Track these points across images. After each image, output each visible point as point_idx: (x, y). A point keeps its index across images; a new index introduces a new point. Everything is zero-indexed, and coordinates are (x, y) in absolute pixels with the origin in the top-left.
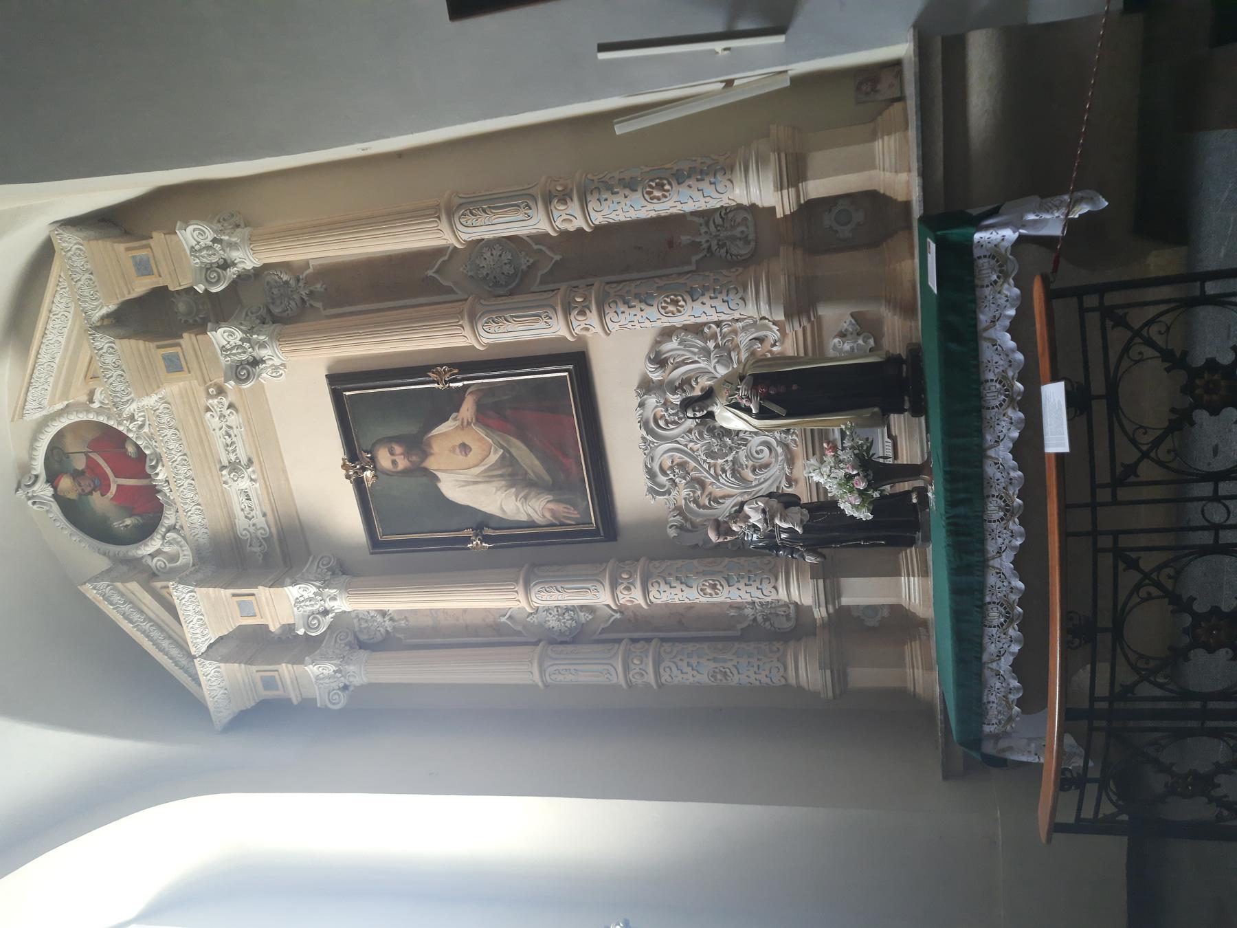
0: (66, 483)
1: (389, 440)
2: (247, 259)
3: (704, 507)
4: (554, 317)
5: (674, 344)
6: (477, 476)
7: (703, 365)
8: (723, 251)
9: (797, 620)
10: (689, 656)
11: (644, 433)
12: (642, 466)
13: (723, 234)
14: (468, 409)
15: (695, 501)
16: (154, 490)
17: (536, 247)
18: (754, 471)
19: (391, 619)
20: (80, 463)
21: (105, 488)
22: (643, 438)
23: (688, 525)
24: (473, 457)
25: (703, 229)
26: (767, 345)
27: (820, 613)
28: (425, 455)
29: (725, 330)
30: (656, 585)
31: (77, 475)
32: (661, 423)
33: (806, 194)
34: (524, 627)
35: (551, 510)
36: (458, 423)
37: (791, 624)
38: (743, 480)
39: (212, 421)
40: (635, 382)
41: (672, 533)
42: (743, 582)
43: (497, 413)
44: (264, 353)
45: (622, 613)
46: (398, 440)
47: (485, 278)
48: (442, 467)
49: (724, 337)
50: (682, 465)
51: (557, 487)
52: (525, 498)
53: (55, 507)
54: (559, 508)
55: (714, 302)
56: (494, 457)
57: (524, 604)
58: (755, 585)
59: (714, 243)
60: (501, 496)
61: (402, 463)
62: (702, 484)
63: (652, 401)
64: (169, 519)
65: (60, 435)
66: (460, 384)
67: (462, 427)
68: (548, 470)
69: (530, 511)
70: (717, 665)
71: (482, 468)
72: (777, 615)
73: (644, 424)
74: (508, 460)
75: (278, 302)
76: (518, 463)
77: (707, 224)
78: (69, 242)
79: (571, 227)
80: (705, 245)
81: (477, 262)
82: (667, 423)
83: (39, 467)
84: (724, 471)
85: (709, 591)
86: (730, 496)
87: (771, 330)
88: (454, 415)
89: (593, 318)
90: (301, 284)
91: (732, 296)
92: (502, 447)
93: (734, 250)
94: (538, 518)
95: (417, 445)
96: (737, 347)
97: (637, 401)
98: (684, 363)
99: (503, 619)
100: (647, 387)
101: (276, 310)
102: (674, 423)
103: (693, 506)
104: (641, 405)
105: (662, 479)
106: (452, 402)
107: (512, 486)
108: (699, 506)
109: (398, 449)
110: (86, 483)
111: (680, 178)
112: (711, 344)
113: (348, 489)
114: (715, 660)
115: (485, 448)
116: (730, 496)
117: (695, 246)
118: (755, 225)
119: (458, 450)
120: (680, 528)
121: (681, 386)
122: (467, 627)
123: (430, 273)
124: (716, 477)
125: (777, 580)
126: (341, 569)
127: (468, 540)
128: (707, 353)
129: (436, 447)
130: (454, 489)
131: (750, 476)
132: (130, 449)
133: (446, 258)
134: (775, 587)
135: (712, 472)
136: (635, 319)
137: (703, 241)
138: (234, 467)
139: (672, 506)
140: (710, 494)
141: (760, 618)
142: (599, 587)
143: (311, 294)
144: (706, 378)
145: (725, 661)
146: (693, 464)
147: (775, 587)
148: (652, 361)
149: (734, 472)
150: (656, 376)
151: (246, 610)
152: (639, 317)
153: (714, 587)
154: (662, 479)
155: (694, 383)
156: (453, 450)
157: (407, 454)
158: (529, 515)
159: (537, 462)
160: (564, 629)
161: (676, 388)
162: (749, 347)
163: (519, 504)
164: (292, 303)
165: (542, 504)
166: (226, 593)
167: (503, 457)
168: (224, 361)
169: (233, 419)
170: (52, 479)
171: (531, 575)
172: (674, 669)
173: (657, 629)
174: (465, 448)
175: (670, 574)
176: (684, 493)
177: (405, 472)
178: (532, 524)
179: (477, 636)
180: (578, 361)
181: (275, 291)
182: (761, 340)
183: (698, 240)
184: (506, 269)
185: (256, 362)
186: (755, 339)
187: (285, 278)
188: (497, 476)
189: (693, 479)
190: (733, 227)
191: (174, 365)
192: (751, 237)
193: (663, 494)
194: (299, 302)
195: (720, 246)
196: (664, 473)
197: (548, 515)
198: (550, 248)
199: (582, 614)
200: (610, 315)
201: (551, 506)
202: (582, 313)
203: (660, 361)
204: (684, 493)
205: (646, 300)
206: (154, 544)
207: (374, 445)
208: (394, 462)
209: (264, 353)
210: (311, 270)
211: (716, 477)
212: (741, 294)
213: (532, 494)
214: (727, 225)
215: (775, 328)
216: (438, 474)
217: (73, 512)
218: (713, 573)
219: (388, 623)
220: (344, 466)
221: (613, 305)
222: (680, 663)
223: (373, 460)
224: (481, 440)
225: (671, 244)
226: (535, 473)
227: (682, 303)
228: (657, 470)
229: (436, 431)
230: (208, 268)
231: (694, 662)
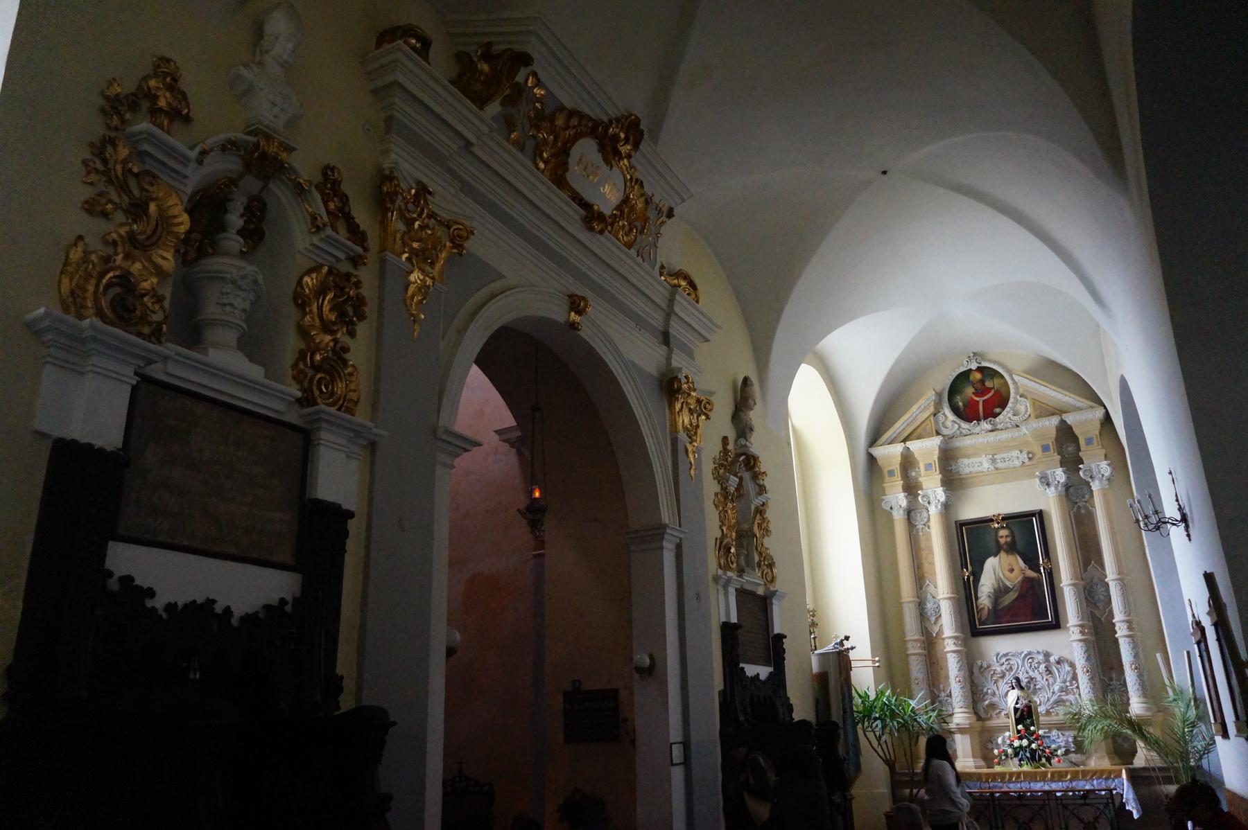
0: (978, 376)
1: (1012, 535)
2: (1095, 486)
5: (1068, 668)
16: (979, 420)
20: (988, 384)
21: (976, 394)
27: (952, 726)
28: (1007, 552)
31: (982, 382)
39: (1015, 453)
40: (1049, 650)
41: (979, 663)
43: (1030, 589)
44: (1053, 488)
46: (1013, 537)
51: (997, 612)
53: (963, 369)
54: (985, 612)
56: (1008, 584)
61: (1002, 541)
62: (1003, 677)
63: (1041, 657)
64: (965, 425)
65: (1002, 377)
73: (1030, 653)
78: (1100, 413)
83: (984, 364)
89: (1079, 637)
94: (980, 601)
95: (1011, 548)
100: (1047, 655)
101: (1071, 490)
110: (979, 386)
111: (1140, 676)
117: (1111, 679)
126: (947, 507)
128: (1064, 682)
129: (1011, 557)
130: (991, 564)
132: (998, 410)
138: (994, 461)
150: (1052, 659)
151: (928, 467)
157: (1006, 543)
159: (1006, 603)
166: (936, 458)
168: (1048, 472)
169: (1017, 463)
170: (980, 369)
171: (956, 602)
174: (1012, 570)
176: (999, 669)
178: (977, 598)
185: (1048, 485)
191: (1045, 448)
200: (1080, 644)
203: (1058, 662)
204: (999, 669)
205: (1088, 659)
206: (951, 416)
209: (1053, 488)
217: (964, 377)
225: (1112, 669)
230: (1090, 470)
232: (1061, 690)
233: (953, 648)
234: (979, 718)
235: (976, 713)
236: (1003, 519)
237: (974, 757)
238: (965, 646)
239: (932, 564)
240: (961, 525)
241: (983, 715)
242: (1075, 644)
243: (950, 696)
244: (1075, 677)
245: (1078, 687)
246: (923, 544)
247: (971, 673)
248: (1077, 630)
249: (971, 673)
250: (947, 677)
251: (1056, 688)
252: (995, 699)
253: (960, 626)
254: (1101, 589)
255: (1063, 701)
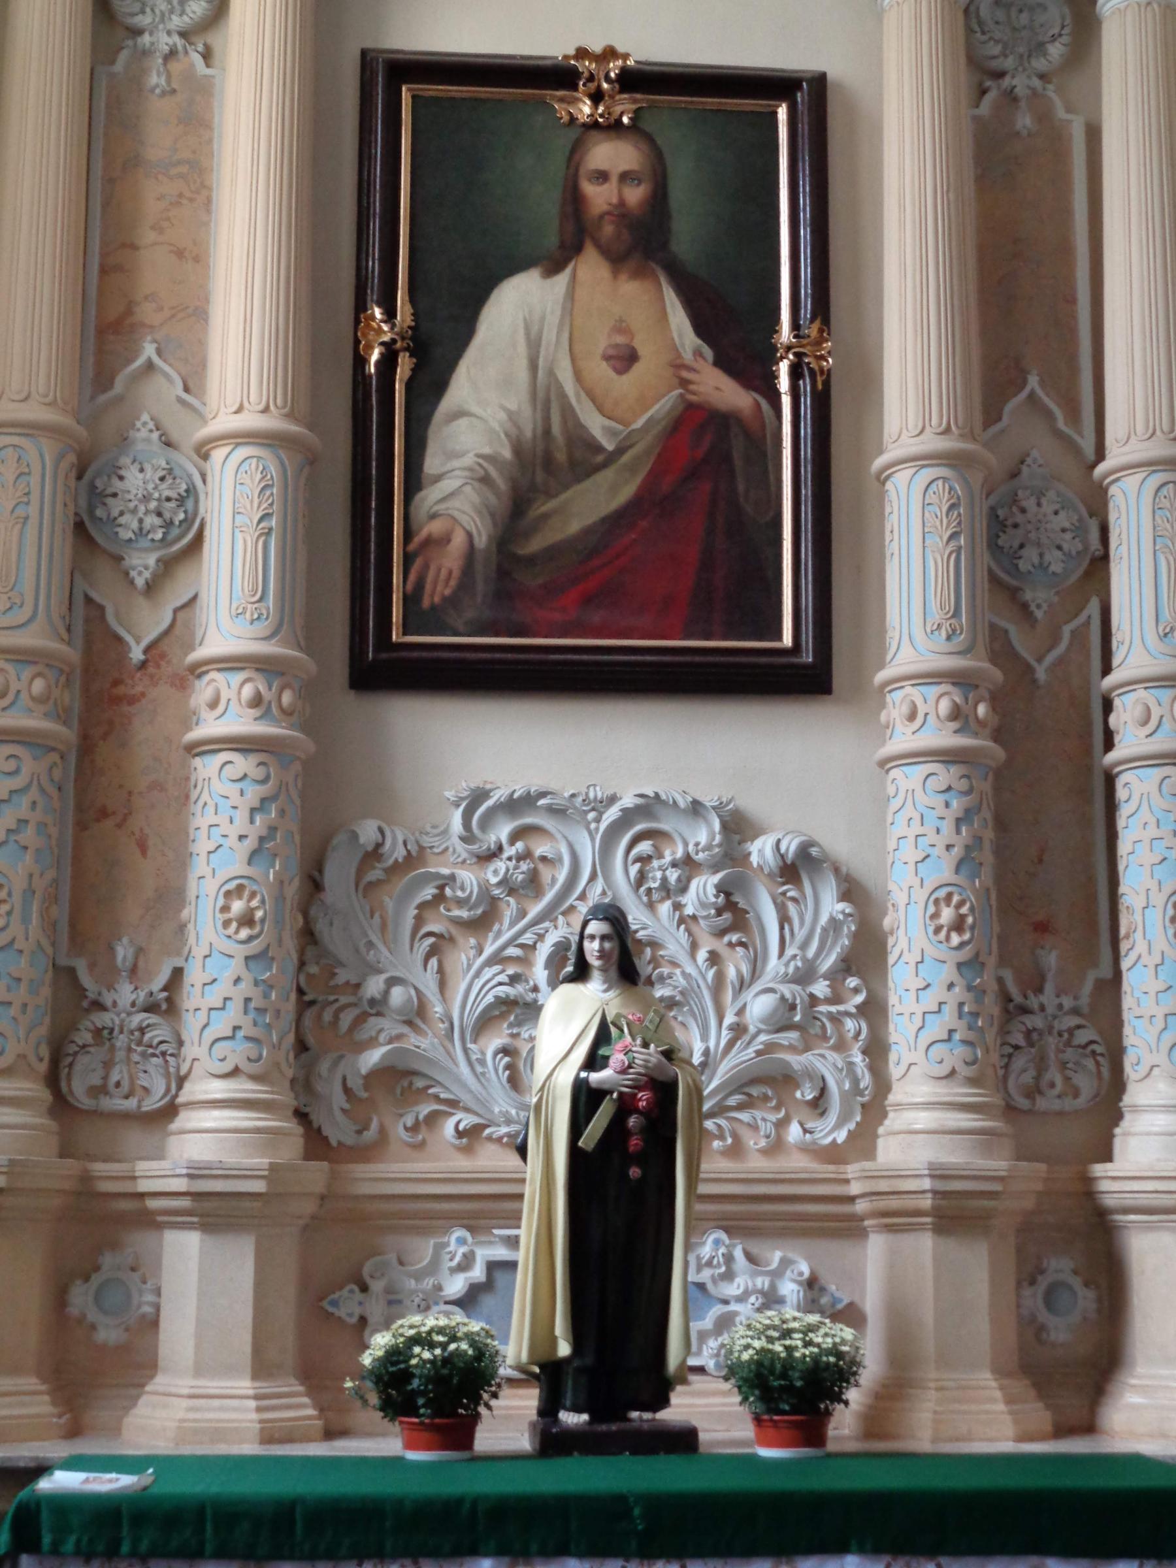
3: (419, 921)
4: (949, 647)
5: (832, 906)
6: (551, 373)
7: (773, 964)
8: (1018, 1039)
9: (96, 1114)
10: (42, 826)
11: (628, 801)
12: (553, 786)
13: (1052, 1041)
14: (725, 392)
15: (440, 898)
17: (1067, 630)
18: (505, 1051)
19: (172, 54)
22: (613, 799)
23: (375, 874)
24: (601, 371)
25: (1067, 1002)
26: (805, 1112)
28: (616, 259)
29: (850, 1025)
30: (259, 773)
32: (644, 847)
33: (1149, 1227)
34: (120, 399)
35: (446, 539)
36: (688, 356)
37: (83, 1100)
38: (485, 1022)
41: (368, 832)
42: (255, 993)
45: (143, 665)
46: (659, 198)
47: (1015, 501)
48: (581, 293)
49: (836, 1019)
50: (533, 884)
51: (509, 568)
52: (485, 480)
54: (451, 560)
55: (949, 1011)
56: (596, 425)
57: (224, 422)
58: (246, 1022)
59: (1036, 1021)
60: (496, 418)
61: (599, 197)
62: (482, 923)
63: (703, 836)
66: (784, 384)
67: (678, 365)
68: (553, 552)
69: (448, 485)
70: (17, 898)
71: (570, 387)
72: (108, 1065)
73: (649, 806)
74: (585, 459)
75: (1000, 15)
76: (579, 480)
77: (1075, 1011)
79: (1124, 716)
80: (1033, 1002)
81: (1051, 494)
82: (644, 860)
84: (514, 979)
85: (237, 906)
86: (442, 985)
87: (838, 1126)
88: (708, 353)
90: (1036, 83)
91: (960, 1051)
92: (620, 451)
93: (1019, 1062)
94: (429, 497)
95: (643, 242)
96: (807, 1049)
97: (709, 800)
98: (784, 919)
99: (149, 350)
100: (737, 828)
102: (642, 878)
103: (428, 892)
104: (696, 808)
105: (502, 831)
106: (747, 358)
107: (518, 450)
108: (422, 906)
109: (635, 195)
112: (820, 988)
113: (547, 43)
114: (30, 891)
115: (626, 410)
116: (442, 985)
118: (1061, 1114)
119: (620, 339)
120: (374, 854)
121: (730, 906)
122: (134, 247)
123: (1033, 381)
124: (497, 959)
125: (255, 1078)
127: (390, 314)
128: (804, 977)
129: (630, 288)
131: (495, 1041)
133: (1061, 424)
134: (235, 1072)
135: (512, 951)
136: (929, 829)
137: (1043, 999)
139: (426, 841)
140: (452, 939)
141: (103, 1019)
142: (263, 628)
143: (1011, 96)
144: (745, 969)
145: (26, 920)
146: (535, 910)
147: (235, 1072)
148: (804, 852)
149: (506, 1005)
150: (761, 851)
152: (932, 838)
153: (247, 920)
154: (502, 831)
155: (734, 938)
156: (621, 327)
157: (621, 212)
158: (438, 478)
159: (574, 526)
160: (115, 506)
161: (728, 895)
162: (811, 1074)
163: (469, 460)
164: (996, 50)
165: (464, 520)
167: (599, 449)
172: (17, 782)
173: (86, 748)
174: (625, 359)
175: (282, 813)
176: (468, 878)
177: (574, 200)
178: (414, 483)
179: (104, 271)
180: (804, 678)
181: (1024, 18)
182: (818, 1104)
183: (1049, 987)
184: (1030, 555)
186: (823, 1091)
187: (1056, 51)
188: (547, 419)
189: (494, 901)
190: (1063, 1065)
192: (1042, 1104)
193: (467, 824)
194: (995, 64)
195: (1028, 1033)
196: (514, 838)
197: (435, 528)
198: (1060, 661)
199: (151, 560)
200: (945, 775)
201: (459, 540)
202: (956, 714)
203: (794, 869)
207: (650, 139)
208: (602, 176)
210: (1061, 114)
211: (497, 959)
212: (965, 1071)
213: (493, 500)
214: (1069, 1054)
215: (841, 1136)
216: (562, 280)
218: (279, 923)
219: (164, 42)
220: (610, 53)
221: (963, 785)
222: (25, 801)
223: (614, 127)
224: (644, 403)
225: (1042, 928)
226: (546, 517)
227: (955, 939)
228: (528, 820)
229: (670, 296)
231: (28, 835)
232: (781, 1019)
233: (238, 721)
234: (316, 1144)
235: (301, 1116)
236: (636, 80)
237: (261, 1368)
238: (306, 727)
239: (194, 256)
240: (393, 72)
241: (338, 1130)
242: (907, 779)
243: (167, 1004)
244: (866, 954)
245: (874, 1010)
246: (159, 138)
247: (314, 884)
248: (937, 702)
249: (314, 884)
250: (171, 896)
251: (759, 1006)
252: (424, 1043)
253: (297, 614)
254: (1055, 519)
255: (785, 1080)
